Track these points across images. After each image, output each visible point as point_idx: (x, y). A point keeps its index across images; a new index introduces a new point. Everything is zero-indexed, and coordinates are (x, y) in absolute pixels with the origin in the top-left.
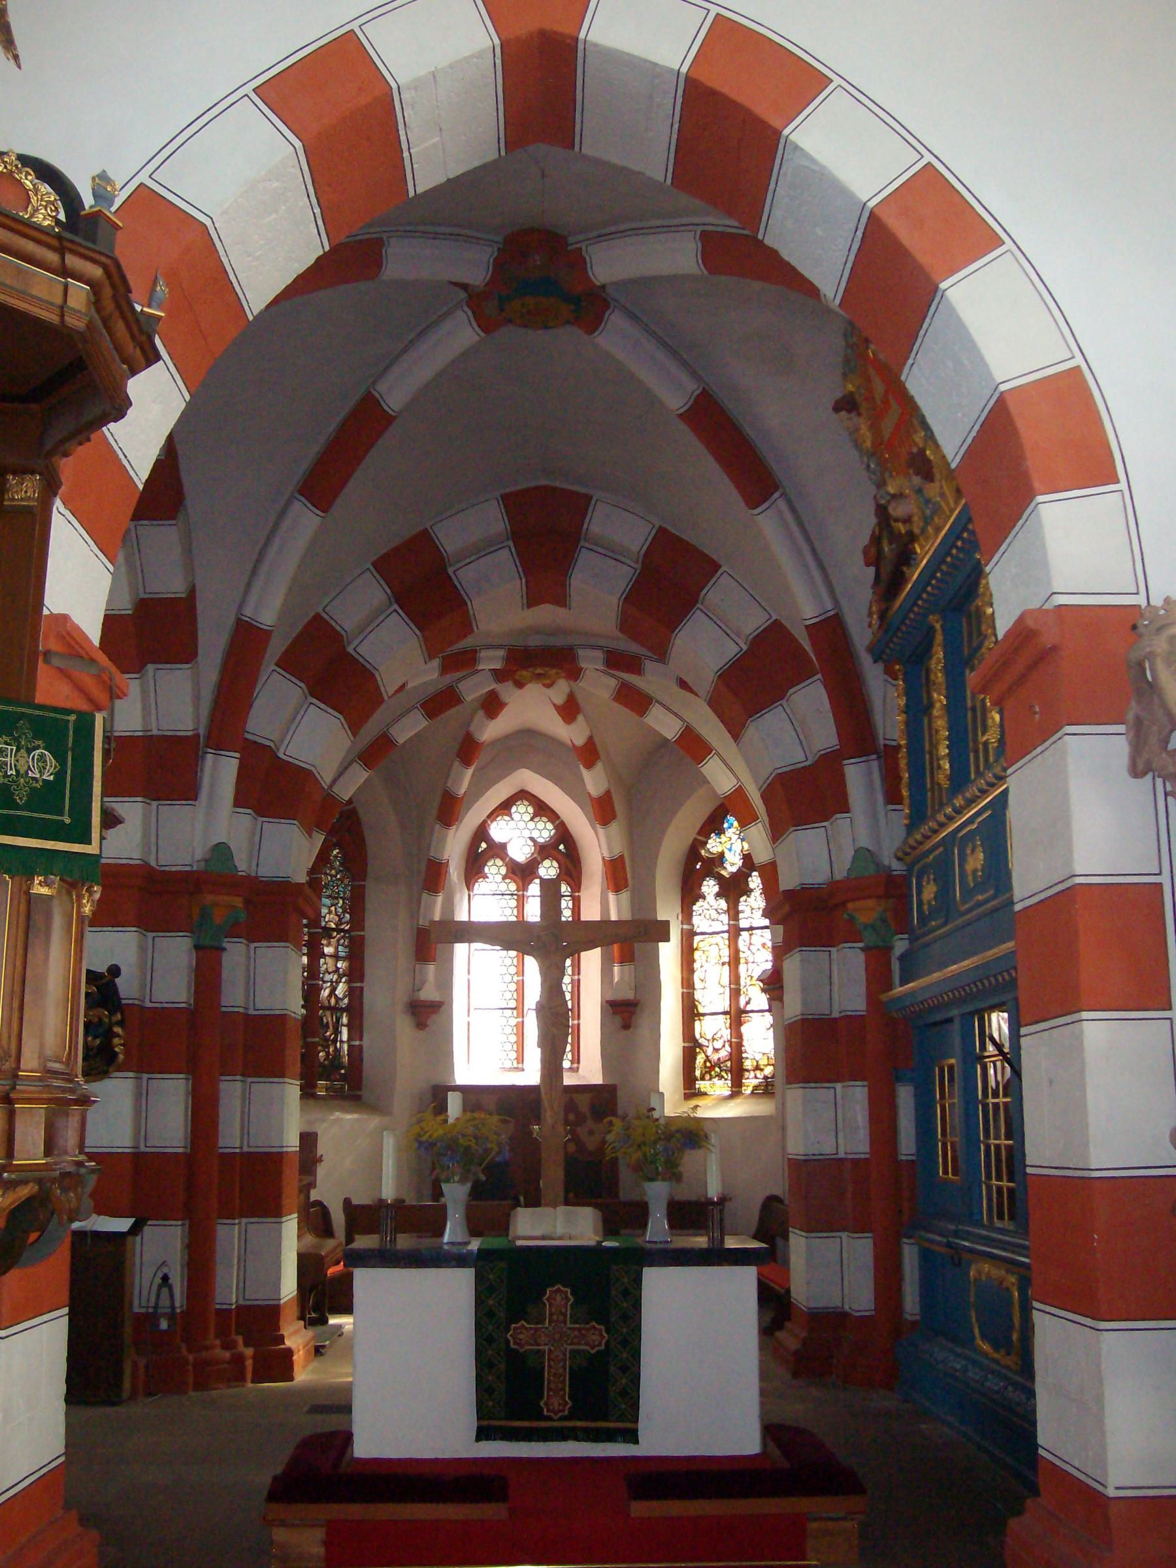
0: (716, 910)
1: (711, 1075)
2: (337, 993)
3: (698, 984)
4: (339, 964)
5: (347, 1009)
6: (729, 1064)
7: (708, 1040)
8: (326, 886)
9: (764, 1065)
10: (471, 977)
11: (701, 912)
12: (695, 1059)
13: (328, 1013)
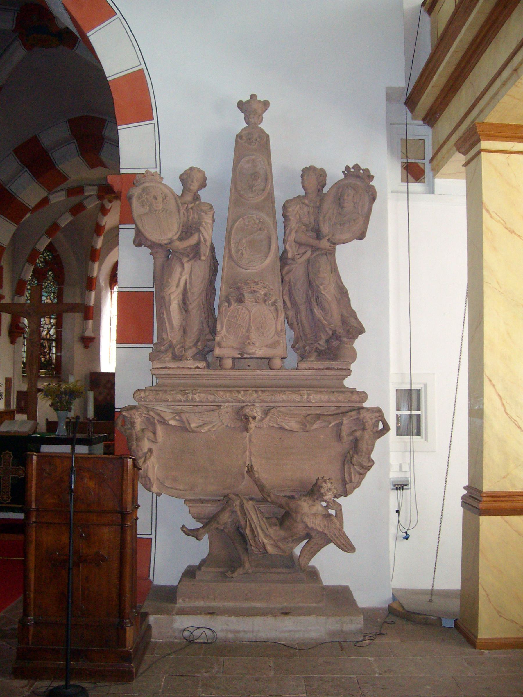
2: (50, 333)
4: (52, 321)
5: (55, 340)
8: (45, 288)
10: (111, 326)
13: (46, 342)
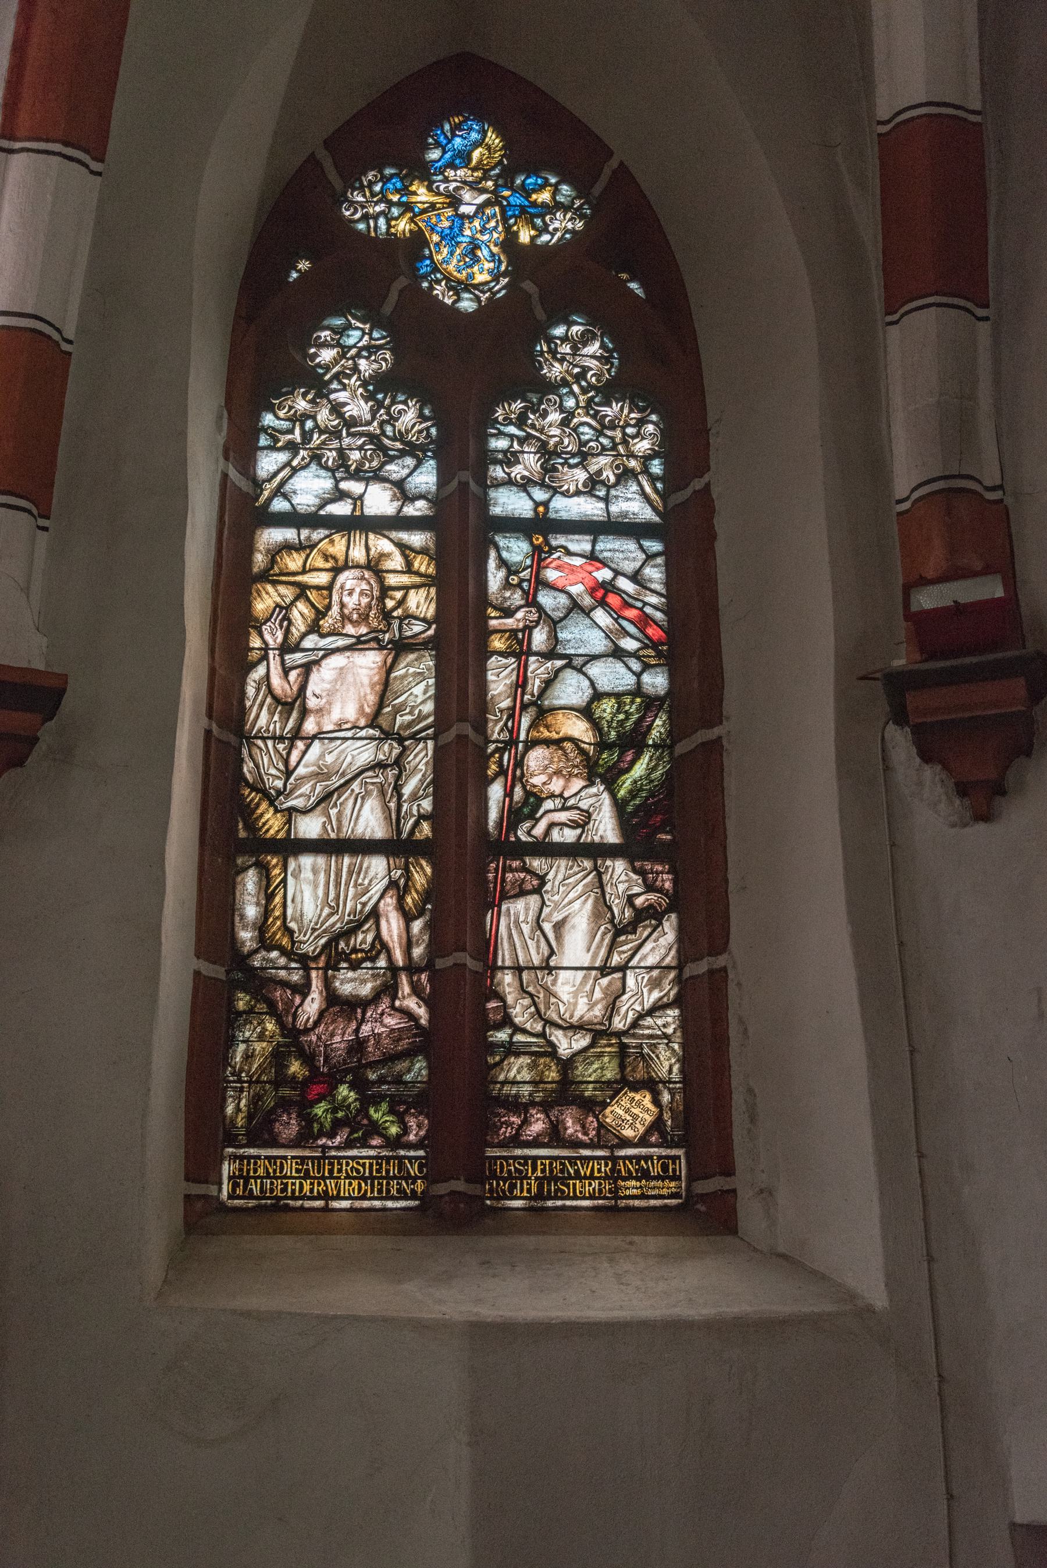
0: (372, 438)
1: (308, 1120)
3: (263, 719)
6: (418, 1069)
7: (305, 961)
9: (602, 1084)
11: (297, 436)
12: (231, 1042)
